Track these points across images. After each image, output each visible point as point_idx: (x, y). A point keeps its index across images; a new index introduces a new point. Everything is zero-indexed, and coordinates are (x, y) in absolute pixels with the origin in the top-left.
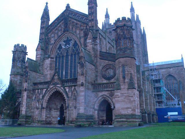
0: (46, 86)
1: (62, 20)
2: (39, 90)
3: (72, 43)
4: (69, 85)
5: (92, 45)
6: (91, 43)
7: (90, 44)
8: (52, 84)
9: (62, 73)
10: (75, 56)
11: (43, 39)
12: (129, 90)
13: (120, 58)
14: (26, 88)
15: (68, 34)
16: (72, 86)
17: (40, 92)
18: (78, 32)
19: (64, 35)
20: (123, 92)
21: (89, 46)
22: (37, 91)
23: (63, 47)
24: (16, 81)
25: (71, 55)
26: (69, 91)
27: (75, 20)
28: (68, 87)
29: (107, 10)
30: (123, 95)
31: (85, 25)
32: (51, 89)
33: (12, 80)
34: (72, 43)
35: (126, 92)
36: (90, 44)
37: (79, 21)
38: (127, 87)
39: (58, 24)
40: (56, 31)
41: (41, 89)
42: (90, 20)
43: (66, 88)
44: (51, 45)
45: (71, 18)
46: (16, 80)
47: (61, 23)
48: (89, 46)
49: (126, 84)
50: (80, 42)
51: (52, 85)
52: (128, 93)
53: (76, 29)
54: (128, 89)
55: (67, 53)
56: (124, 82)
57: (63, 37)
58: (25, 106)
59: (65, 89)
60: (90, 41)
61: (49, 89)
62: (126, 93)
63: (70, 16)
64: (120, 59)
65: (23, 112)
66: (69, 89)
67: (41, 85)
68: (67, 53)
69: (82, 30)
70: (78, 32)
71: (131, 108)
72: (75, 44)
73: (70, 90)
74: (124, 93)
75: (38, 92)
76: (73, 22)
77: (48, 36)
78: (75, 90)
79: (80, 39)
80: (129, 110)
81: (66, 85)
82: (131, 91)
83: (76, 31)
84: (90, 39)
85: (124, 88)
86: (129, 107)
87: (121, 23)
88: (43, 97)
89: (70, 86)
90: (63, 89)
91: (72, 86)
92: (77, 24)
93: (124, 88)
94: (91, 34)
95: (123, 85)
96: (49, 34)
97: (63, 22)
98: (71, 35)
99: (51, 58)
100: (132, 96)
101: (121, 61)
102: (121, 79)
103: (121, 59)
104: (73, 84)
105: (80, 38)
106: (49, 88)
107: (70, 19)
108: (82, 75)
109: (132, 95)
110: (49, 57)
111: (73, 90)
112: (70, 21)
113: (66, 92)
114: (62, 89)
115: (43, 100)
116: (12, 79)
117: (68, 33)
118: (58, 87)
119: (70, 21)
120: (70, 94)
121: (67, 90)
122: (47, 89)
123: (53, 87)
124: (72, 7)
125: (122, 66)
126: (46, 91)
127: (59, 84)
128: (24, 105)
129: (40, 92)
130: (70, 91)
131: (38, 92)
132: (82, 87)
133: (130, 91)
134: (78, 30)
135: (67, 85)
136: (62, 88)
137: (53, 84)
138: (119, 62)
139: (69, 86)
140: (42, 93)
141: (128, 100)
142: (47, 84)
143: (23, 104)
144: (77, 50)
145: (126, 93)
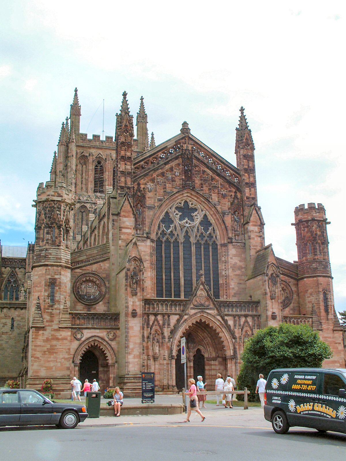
0: (178, 310)
1: (177, 158)
2: (159, 317)
3: (198, 218)
4: (234, 313)
5: (259, 239)
6: (258, 234)
7: (257, 236)
8: (192, 306)
9: (177, 280)
10: (207, 249)
11: (129, 188)
12: (335, 332)
13: (320, 276)
14: (134, 310)
15: (192, 194)
16: (239, 316)
17: (161, 322)
18: (215, 198)
19: (183, 194)
20: (326, 335)
21: (253, 238)
22: (152, 318)
23: (177, 222)
24: (66, 283)
25: (198, 244)
26: (235, 326)
27: (211, 169)
28: (230, 317)
29: (76, 95)
30: (327, 340)
31: (234, 190)
32: (191, 316)
33: (55, 279)
34: (198, 218)
35: (331, 335)
36: (257, 236)
37: (218, 175)
38: (332, 327)
39: (166, 164)
40: (160, 179)
41: (163, 315)
42: (247, 183)
43: (226, 318)
44: (150, 208)
45: (198, 159)
46: (65, 281)
47: (173, 164)
48: (253, 238)
49: (330, 322)
50: (224, 222)
51: (192, 308)
52: (333, 338)
53: (210, 189)
54: (334, 330)
55: (187, 237)
56: (328, 319)
57: (179, 197)
58: (137, 351)
59: (226, 321)
60: (256, 229)
61: (186, 317)
62: (330, 338)
63: (196, 154)
64: (319, 278)
65: (131, 366)
66: (235, 321)
67: (162, 305)
68: (187, 237)
69: (224, 196)
70: (215, 198)
71: (338, 362)
72: (206, 223)
73: (237, 322)
74: (327, 337)
75: (156, 320)
76: (204, 172)
77: (139, 184)
78: (246, 324)
79: (224, 216)
80: (336, 364)
81: (226, 313)
82: (337, 335)
83: (211, 195)
84: (255, 226)
85: (328, 329)
86: (336, 360)
87: (318, 214)
88: (173, 332)
89: (238, 315)
90: (220, 319)
91: (239, 316)
92: (213, 179)
93: (328, 329)
94: (257, 215)
95: (325, 322)
96: (142, 181)
97: (177, 162)
98: (198, 198)
99: (151, 241)
100: (340, 343)
101: (322, 283)
102: (323, 313)
103: (322, 278)
104: (243, 313)
105: (224, 214)
106: (185, 315)
107: (195, 161)
108: (272, 299)
109: (340, 342)
110: (148, 238)
111: (242, 323)
112: (196, 166)
113: (228, 327)
114: (219, 321)
115: (171, 340)
116: (56, 277)
117: (193, 193)
118: (210, 314)
119: (197, 166)
120: (237, 332)
121: (231, 323)
122: (181, 316)
123: (195, 314)
124: (195, 132)
125: (323, 291)
126: (178, 321)
127: (211, 309)
128: (133, 349)
129: (161, 322)
130: (237, 325)
131: (156, 320)
132: (273, 321)
133: (336, 334)
134: (215, 193)
135: (230, 313)
136: (219, 318)
137: (196, 307)
138: (318, 284)
139: (234, 316)
140: (169, 325)
141: (333, 349)
142: (180, 305)
143: (131, 346)
144: (210, 236)
145: (330, 338)
